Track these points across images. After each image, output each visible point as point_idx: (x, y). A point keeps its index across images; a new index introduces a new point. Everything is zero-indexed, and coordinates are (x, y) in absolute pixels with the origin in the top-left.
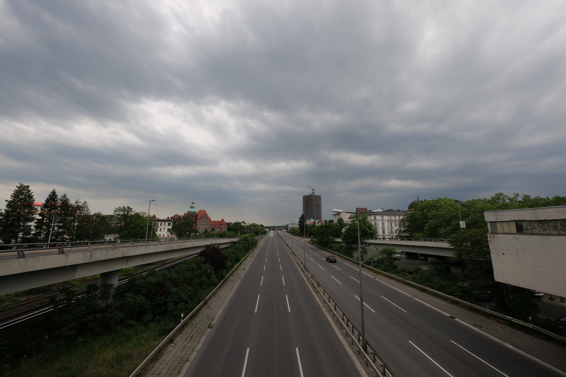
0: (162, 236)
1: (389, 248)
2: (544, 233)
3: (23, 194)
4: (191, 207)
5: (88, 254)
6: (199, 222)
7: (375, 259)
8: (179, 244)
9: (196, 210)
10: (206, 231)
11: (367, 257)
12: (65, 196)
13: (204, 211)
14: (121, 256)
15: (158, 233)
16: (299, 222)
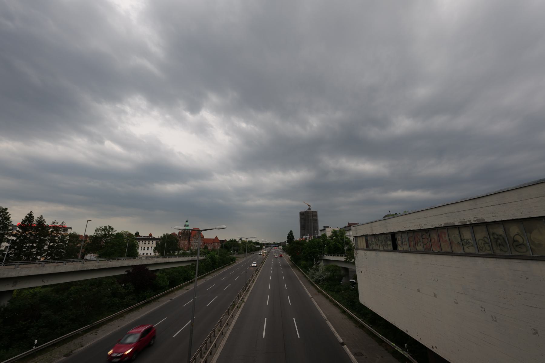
0: (145, 254)
2: (378, 248)
4: (186, 226)
6: (192, 240)
8: (97, 264)
9: (191, 227)
12: (41, 217)
15: (140, 252)
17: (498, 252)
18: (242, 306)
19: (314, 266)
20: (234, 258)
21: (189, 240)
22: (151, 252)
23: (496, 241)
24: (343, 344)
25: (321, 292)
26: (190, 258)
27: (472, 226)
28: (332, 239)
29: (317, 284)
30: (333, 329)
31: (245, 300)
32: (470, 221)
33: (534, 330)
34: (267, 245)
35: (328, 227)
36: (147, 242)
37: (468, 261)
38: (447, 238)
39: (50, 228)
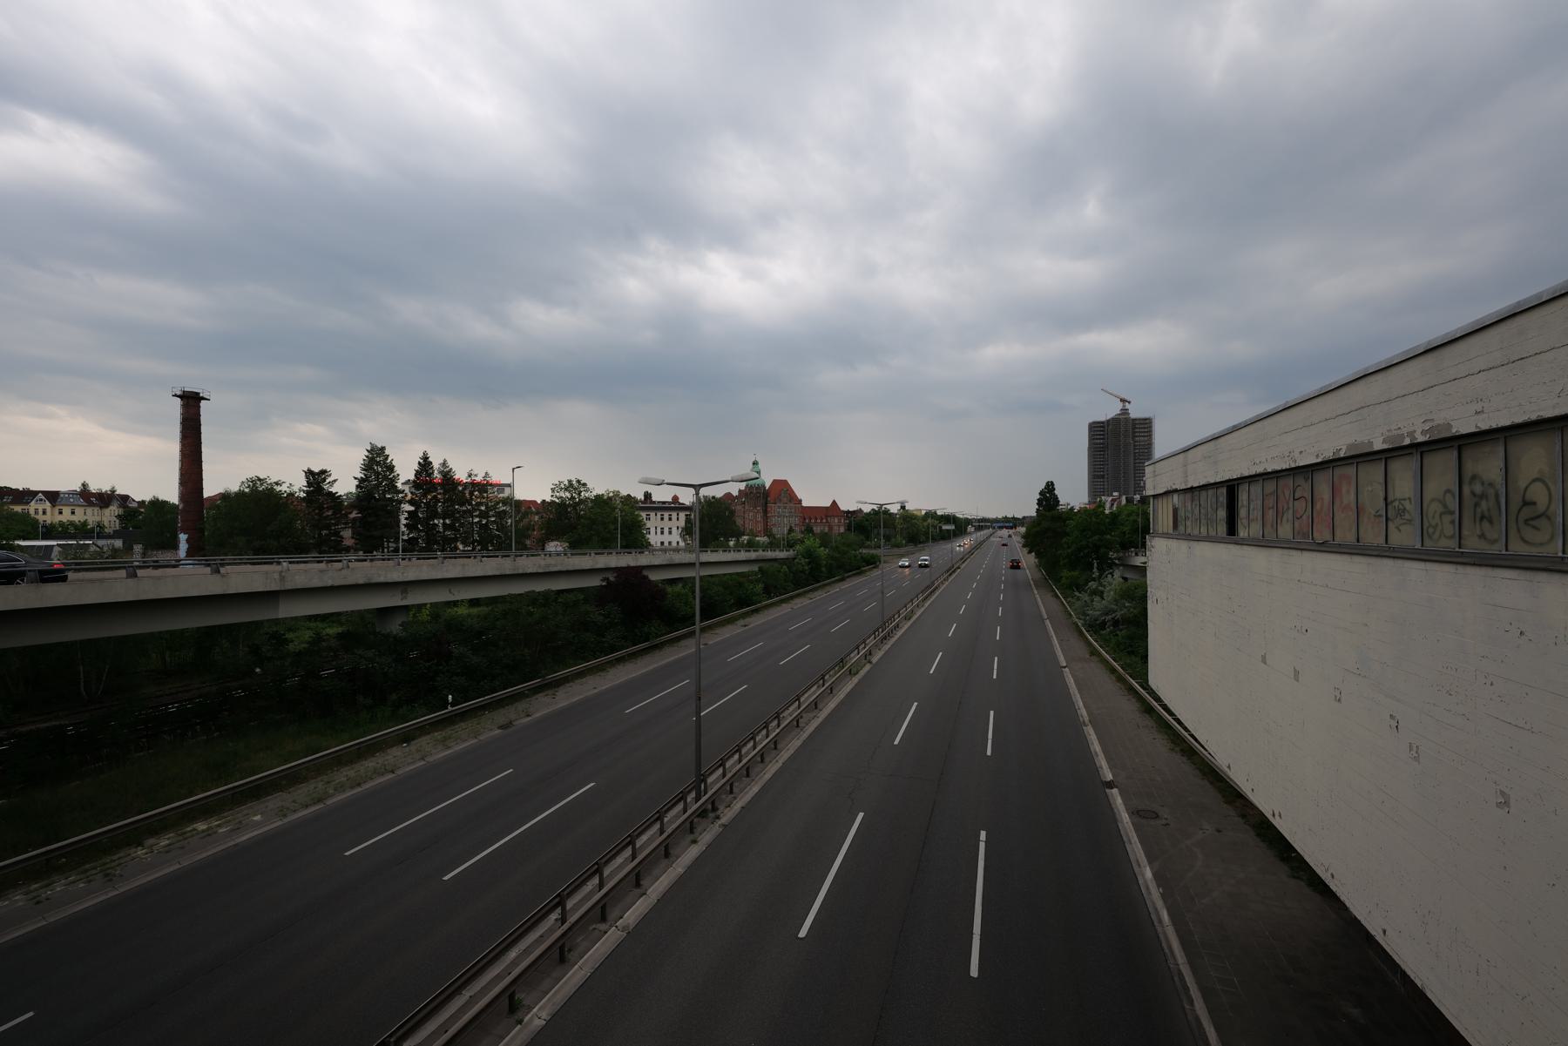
3: (378, 463)
5: (276, 576)
6: (775, 509)
7: (1118, 615)
12: (444, 464)
13: (785, 483)
14: (361, 581)
15: (654, 539)
17: (1473, 544)
18: (862, 673)
19: (1092, 585)
21: (765, 512)
22: (675, 538)
23: (1476, 505)
24: (1110, 785)
25: (1099, 655)
26: (753, 555)
27: (1420, 449)
30: (1096, 747)
31: (875, 660)
32: (1411, 434)
33: (1503, 793)
34: (982, 524)
36: (666, 515)
37: (1387, 568)
38: (1353, 496)
39: (466, 485)
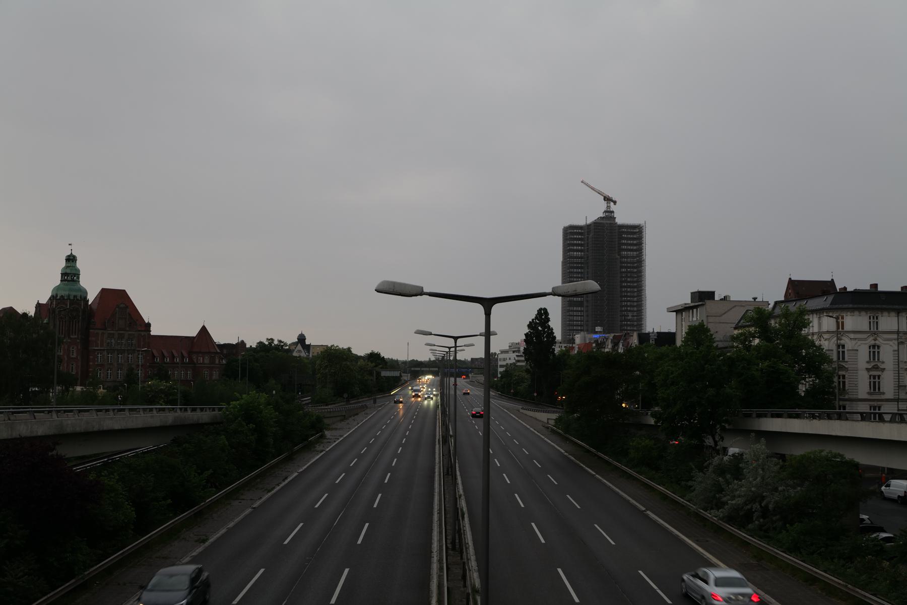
1: (827, 450)
10: (131, 378)
11: (739, 493)
13: (121, 295)
16: (525, 340)
20: (319, 420)
28: (748, 348)
29: (741, 527)
35: (710, 295)
